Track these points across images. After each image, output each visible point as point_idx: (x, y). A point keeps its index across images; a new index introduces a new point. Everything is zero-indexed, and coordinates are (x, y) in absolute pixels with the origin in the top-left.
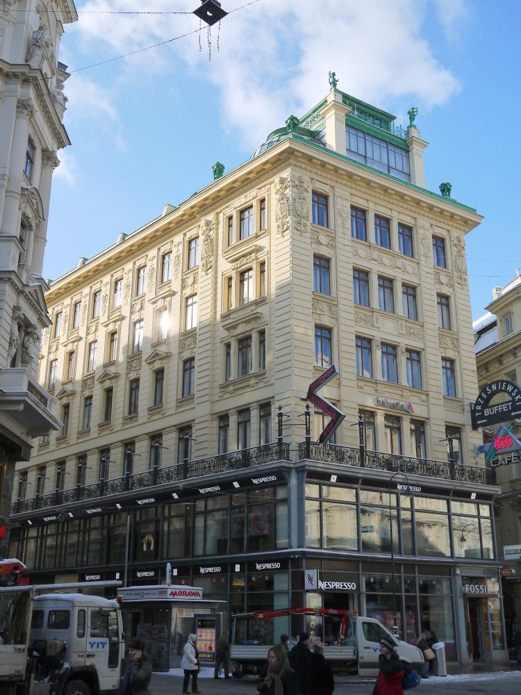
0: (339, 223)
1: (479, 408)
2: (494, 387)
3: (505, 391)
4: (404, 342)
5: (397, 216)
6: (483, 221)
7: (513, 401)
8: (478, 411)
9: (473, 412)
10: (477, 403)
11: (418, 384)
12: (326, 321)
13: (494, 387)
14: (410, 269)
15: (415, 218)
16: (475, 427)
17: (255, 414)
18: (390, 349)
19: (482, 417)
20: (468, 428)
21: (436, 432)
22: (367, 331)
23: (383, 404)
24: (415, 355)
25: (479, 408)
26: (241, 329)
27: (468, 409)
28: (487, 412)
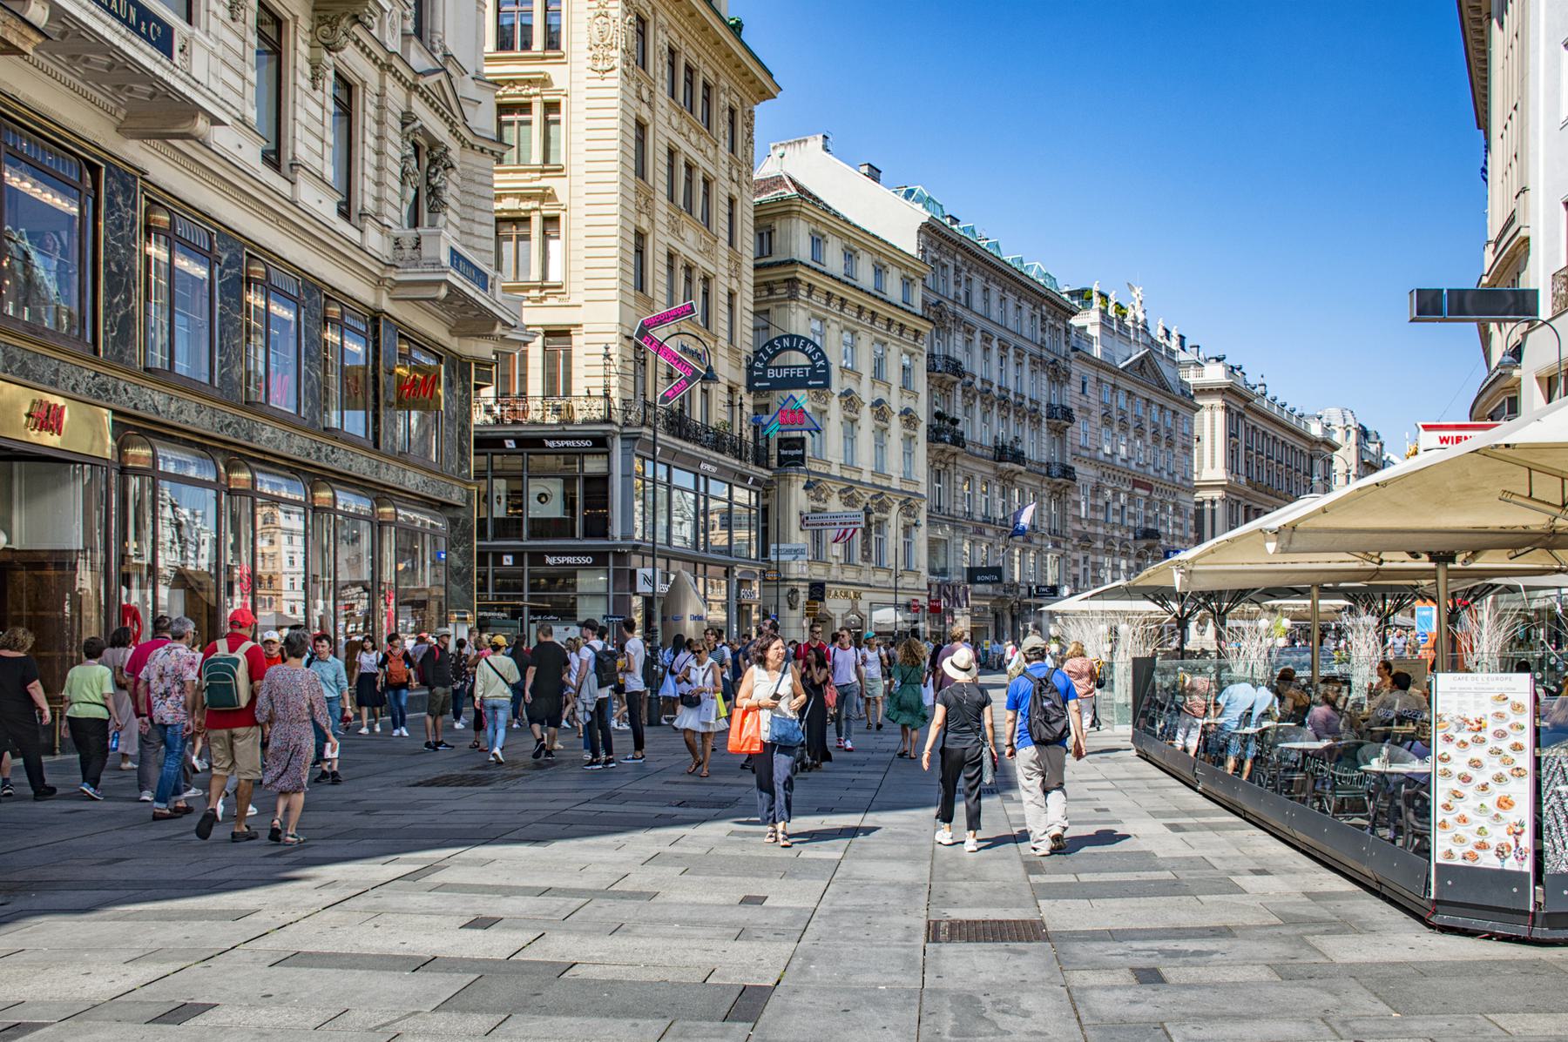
0: (659, 70)
1: (760, 365)
2: (786, 342)
3: (803, 351)
4: (701, 262)
5: (705, 73)
6: (779, 95)
7: (813, 367)
8: (758, 370)
9: (750, 368)
13: (786, 342)
15: (717, 75)
19: (763, 378)
20: (743, 390)
25: (760, 365)
27: (744, 364)
28: (771, 373)
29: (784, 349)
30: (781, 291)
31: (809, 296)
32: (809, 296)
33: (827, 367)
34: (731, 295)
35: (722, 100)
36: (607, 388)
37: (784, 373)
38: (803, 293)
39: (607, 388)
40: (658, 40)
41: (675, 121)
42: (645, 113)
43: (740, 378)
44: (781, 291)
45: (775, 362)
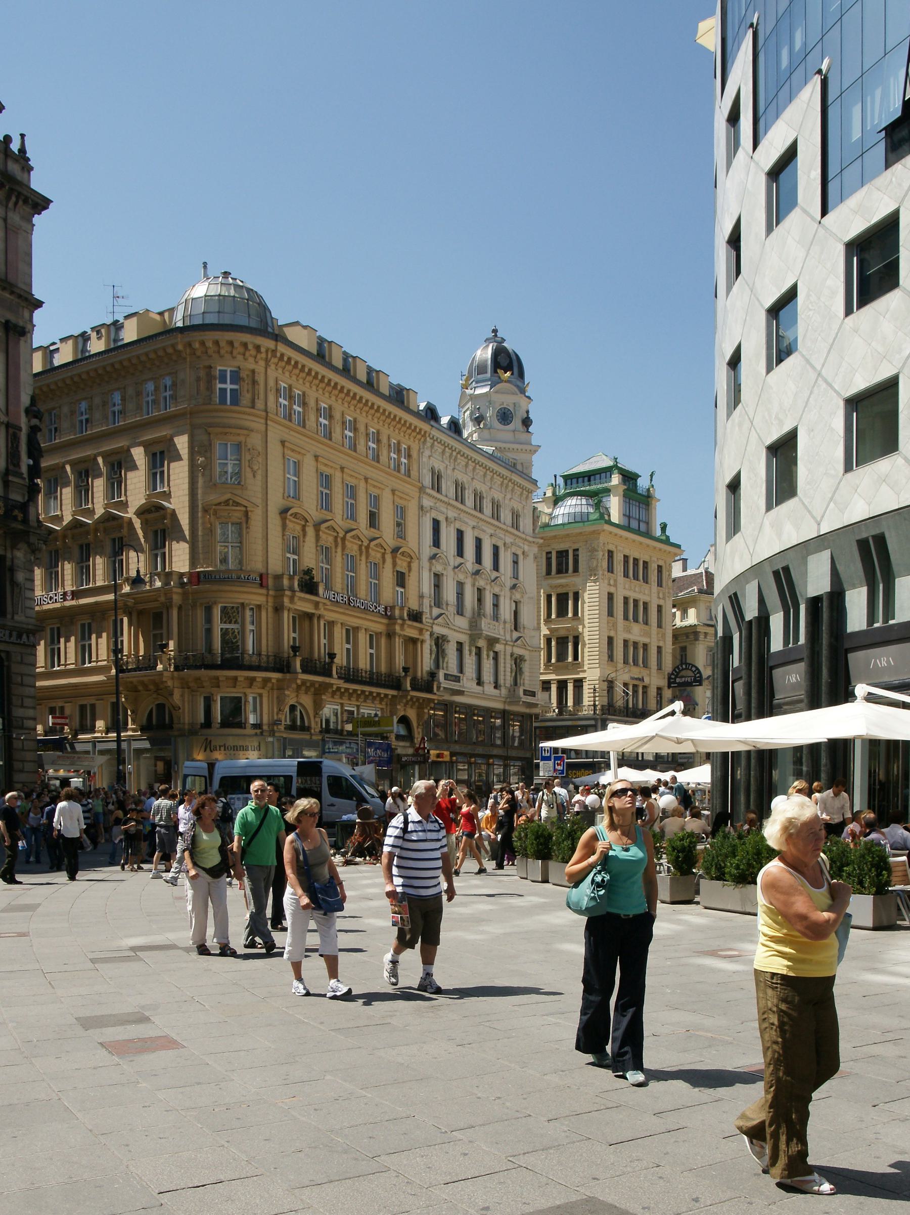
4: (643, 640)
9: (669, 678)
10: (672, 674)
11: (646, 665)
12: (612, 634)
14: (646, 592)
16: (669, 687)
17: (570, 687)
18: (635, 644)
19: (675, 682)
20: (666, 688)
21: (653, 692)
22: (627, 636)
23: (633, 678)
24: (645, 646)
26: (562, 633)
28: (678, 680)
29: (683, 669)
30: (692, 637)
31: (705, 637)
32: (705, 637)
33: (701, 676)
34: (659, 648)
35: (653, 568)
36: (595, 701)
37: (683, 679)
38: (702, 637)
39: (595, 701)
40: (618, 558)
41: (627, 586)
42: (612, 590)
43: (663, 683)
44: (692, 637)
45: (681, 674)
